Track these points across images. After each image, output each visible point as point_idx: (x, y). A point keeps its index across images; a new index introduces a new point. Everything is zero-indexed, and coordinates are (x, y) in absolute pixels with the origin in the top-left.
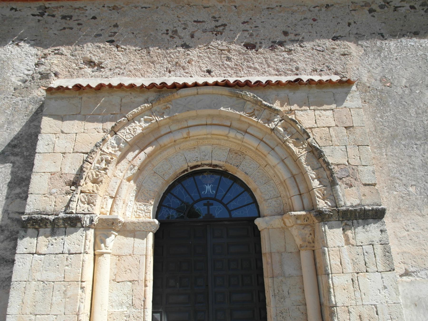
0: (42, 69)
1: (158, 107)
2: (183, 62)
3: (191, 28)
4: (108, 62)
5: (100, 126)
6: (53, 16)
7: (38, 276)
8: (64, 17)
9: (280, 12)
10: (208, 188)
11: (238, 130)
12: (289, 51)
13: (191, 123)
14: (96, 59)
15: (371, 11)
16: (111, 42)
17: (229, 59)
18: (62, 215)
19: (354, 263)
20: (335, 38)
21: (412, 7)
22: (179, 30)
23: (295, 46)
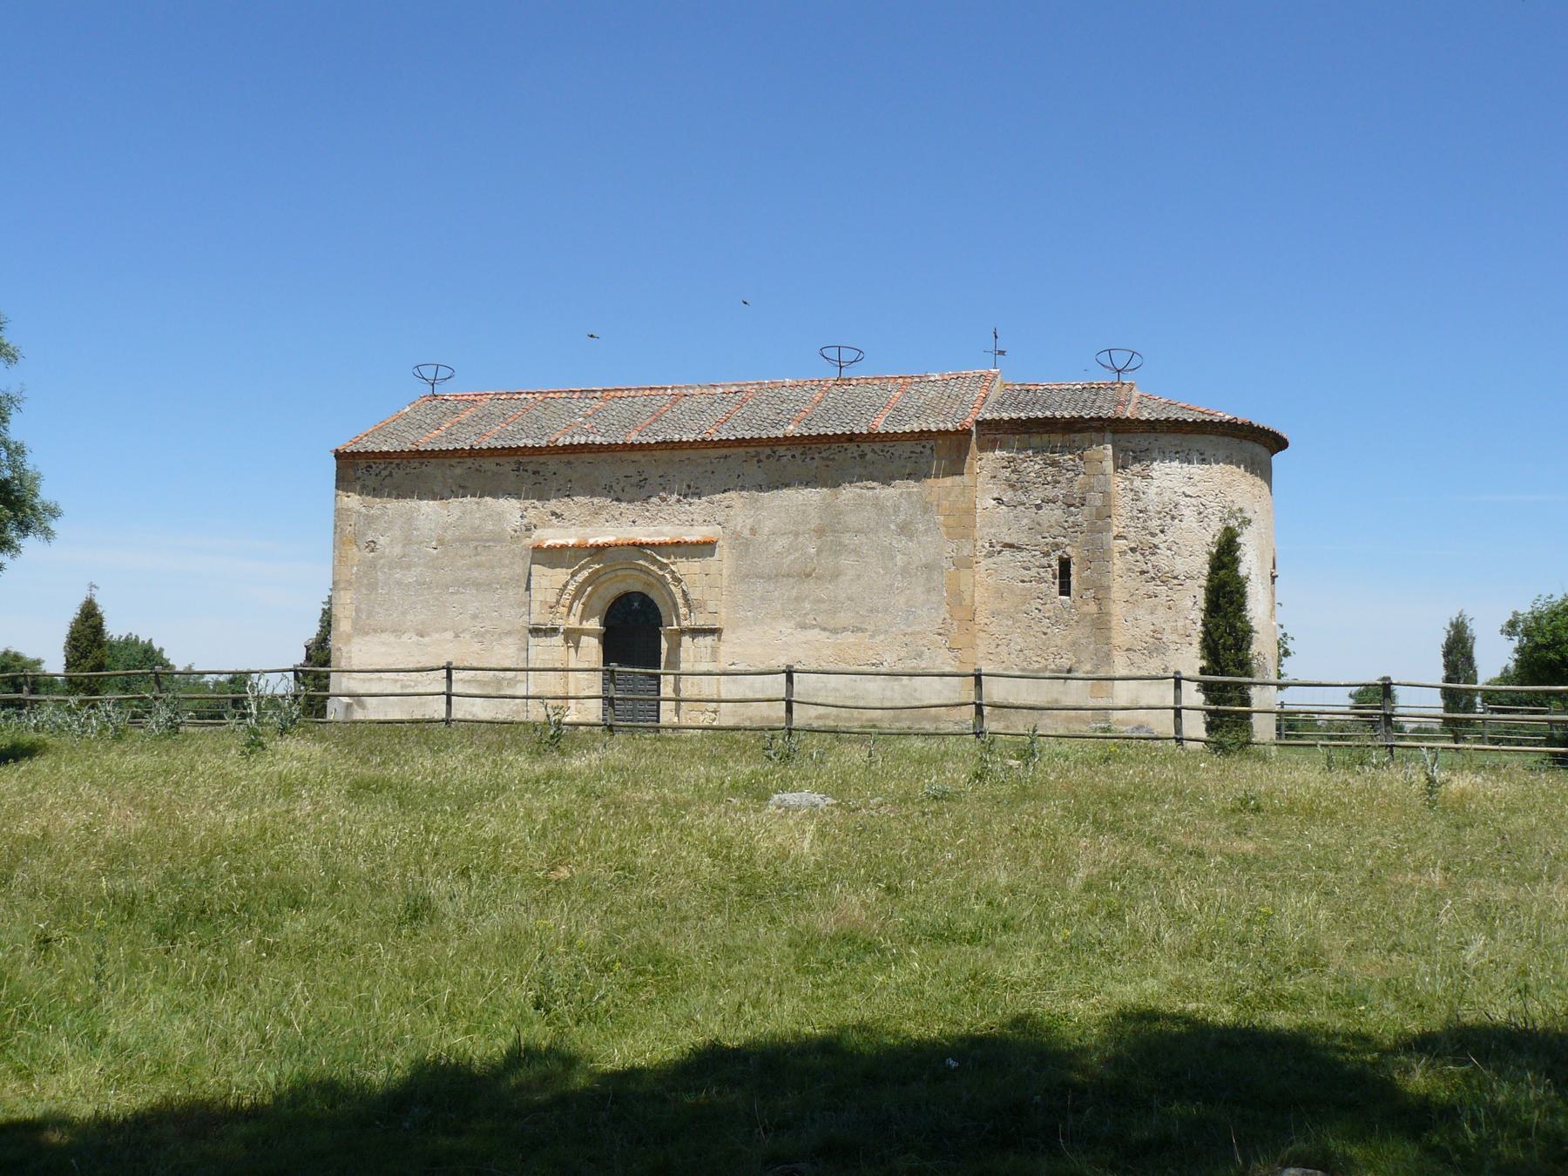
0: (525, 521)
1: (597, 558)
2: (617, 514)
3: (622, 484)
4: (566, 514)
5: (564, 570)
6: (527, 471)
7: (540, 657)
8: (534, 473)
9: (687, 465)
10: (636, 604)
11: (645, 572)
12: (690, 504)
13: (618, 567)
14: (558, 511)
15: (759, 461)
16: (568, 496)
17: (648, 511)
18: (549, 626)
19: (695, 657)
21: (793, 456)
22: (614, 484)
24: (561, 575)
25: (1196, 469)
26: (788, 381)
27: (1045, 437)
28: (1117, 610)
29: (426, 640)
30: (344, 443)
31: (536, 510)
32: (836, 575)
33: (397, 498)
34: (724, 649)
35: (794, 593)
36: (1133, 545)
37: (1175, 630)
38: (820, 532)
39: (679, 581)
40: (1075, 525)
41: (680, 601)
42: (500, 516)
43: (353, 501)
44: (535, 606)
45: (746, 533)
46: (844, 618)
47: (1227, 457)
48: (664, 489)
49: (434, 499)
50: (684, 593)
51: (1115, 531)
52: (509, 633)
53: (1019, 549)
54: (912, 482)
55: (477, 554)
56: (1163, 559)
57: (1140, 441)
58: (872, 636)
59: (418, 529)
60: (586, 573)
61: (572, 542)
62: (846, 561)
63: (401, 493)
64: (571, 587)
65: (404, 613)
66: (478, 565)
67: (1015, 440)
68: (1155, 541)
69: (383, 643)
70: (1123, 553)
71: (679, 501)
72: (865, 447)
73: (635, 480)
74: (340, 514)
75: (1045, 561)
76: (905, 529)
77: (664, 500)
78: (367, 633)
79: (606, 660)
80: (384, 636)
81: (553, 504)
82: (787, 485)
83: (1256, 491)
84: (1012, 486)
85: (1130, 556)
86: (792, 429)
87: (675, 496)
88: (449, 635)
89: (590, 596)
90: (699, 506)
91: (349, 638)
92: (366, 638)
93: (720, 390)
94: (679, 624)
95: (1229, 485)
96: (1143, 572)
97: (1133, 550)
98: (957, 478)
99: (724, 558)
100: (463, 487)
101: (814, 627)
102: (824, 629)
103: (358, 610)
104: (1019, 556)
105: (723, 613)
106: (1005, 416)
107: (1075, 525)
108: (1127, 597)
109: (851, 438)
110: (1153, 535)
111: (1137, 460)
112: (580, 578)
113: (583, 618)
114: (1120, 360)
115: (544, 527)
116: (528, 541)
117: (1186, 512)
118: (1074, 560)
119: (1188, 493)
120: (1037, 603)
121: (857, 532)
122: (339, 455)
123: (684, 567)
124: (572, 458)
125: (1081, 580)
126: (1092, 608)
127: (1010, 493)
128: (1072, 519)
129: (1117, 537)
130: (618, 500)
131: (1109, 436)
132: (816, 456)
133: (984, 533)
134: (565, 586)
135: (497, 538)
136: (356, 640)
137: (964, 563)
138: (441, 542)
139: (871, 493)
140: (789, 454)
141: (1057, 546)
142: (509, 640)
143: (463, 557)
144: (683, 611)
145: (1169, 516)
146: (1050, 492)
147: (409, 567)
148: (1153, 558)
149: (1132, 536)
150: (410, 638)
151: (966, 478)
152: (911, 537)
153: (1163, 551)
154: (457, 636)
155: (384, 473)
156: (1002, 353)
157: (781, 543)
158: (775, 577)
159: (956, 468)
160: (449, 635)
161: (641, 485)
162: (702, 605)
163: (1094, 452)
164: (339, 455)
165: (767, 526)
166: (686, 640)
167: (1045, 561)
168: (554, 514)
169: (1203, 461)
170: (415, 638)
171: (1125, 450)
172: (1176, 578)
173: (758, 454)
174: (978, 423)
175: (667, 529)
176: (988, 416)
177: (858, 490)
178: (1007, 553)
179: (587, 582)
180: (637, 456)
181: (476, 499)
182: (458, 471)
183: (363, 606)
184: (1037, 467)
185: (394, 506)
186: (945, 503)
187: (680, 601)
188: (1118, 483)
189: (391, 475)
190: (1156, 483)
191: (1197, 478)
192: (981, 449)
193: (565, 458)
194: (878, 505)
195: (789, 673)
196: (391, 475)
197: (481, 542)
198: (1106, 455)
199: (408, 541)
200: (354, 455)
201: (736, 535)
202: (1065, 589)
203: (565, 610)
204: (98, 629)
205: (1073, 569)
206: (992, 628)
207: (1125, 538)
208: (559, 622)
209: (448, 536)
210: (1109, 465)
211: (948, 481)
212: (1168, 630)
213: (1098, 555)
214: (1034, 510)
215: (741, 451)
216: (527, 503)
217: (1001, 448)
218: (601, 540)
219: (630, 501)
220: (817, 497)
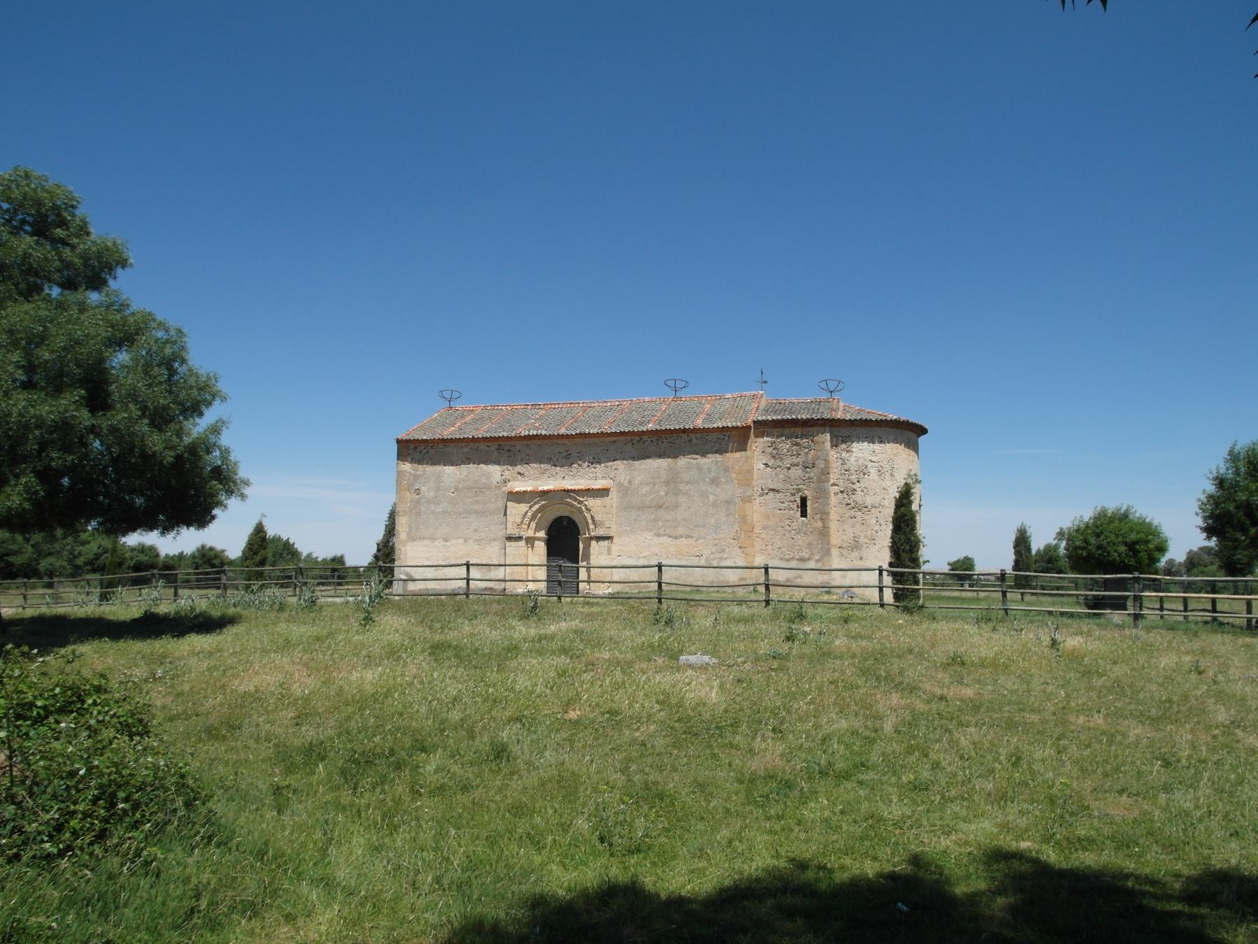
0: (503, 477)
1: (543, 498)
4: (526, 474)
20: (614, 461)
23: (598, 466)
24: (523, 507)
25: (877, 447)
26: (647, 399)
27: (792, 430)
28: (833, 525)
29: (449, 543)
30: (402, 435)
31: (509, 471)
32: (676, 507)
33: (431, 465)
34: (614, 547)
35: (653, 516)
36: (842, 489)
37: (866, 536)
38: (667, 483)
39: (589, 510)
40: (809, 478)
41: (590, 521)
42: (489, 475)
43: (407, 467)
44: (509, 525)
45: (626, 484)
46: (681, 530)
48: (580, 460)
49: (452, 465)
50: (592, 517)
51: (832, 481)
52: (495, 540)
53: (778, 491)
54: (718, 455)
55: (477, 496)
56: (859, 497)
57: (845, 431)
58: (696, 541)
59: (443, 482)
60: (537, 506)
61: (529, 489)
62: (682, 499)
63: (434, 462)
64: (529, 514)
65: (436, 529)
66: (477, 502)
67: (775, 432)
68: (855, 487)
69: (425, 546)
70: (836, 494)
71: (588, 466)
72: (692, 436)
73: (564, 454)
74: (400, 474)
75: (792, 498)
76: (714, 481)
77: (580, 465)
78: (416, 540)
79: (548, 555)
80: (425, 542)
81: (519, 468)
82: (648, 457)
84: (773, 457)
85: (840, 496)
86: (650, 426)
87: (587, 464)
88: (461, 541)
89: (540, 519)
90: (600, 469)
91: (405, 544)
92: (416, 543)
93: (609, 404)
94: (589, 534)
96: (847, 504)
97: (842, 492)
98: (743, 453)
99: (614, 498)
100: (468, 459)
101: (664, 535)
102: (670, 537)
103: (410, 527)
104: (778, 495)
105: (614, 527)
106: (769, 418)
107: (809, 478)
108: (839, 518)
109: (684, 431)
110: (853, 483)
111: (844, 442)
112: (534, 509)
113: (536, 530)
114: (832, 386)
115: (514, 480)
116: (504, 489)
117: (872, 470)
118: (809, 498)
120: (788, 522)
121: (688, 483)
122: (399, 442)
123: (591, 502)
124: (529, 442)
125: (812, 510)
126: (819, 524)
127: (772, 461)
128: (807, 475)
129: (833, 485)
130: (555, 466)
131: (828, 429)
132: (665, 441)
133: (757, 484)
134: (526, 513)
135: (488, 487)
136: (409, 544)
137: (747, 500)
138: (457, 489)
139: (695, 461)
140: (650, 440)
141: (799, 490)
142: (495, 543)
143: (469, 498)
144: (592, 527)
146: (795, 460)
147: (438, 504)
148: (853, 496)
149: (841, 482)
150: (438, 543)
151: (748, 453)
152: (717, 486)
153: (859, 492)
154: (466, 541)
155: (424, 451)
156: (765, 382)
157: (645, 489)
158: (642, 508)
159: (742, 447)
160: (461, 541)
161: (568, 456)
162: (602, 523)
163: (819, 438)
164: (399, 442)
165: (638, 480)
166: (593, 543)
167: (792, 498)
168: (519, 473)
169: (881, 442)
170: (442, 542)
171: (837, 437)
172: (866, 507)
173: (632, 440)
174: (754, 422)
175: (582, 481)
176: (760, 418)
177: (688, 460)
178: (771, 494)
179: (538, 511)
180: (565, 441)
181: (475, 466)
182: (466, 450)
183: (413, 525)
184: (788, 446)
185: (430, 469)
186: (737, 467)
187: (590, 521)
188: (833, 454)
189: (428, 452)
192: (756, 436)
193: (525, 442)
194: (699, 468)
195: (660, 567)
196: (428, 452)
197: (480, 489)
198: (826, 440)
199: (438, 489)
200: (408, 441)
201: (620, 485)
202: (804, 514)
203: (525, 527)
204: (264, 539)
205: (809, 503)
206: (763, 536)
207: (837, 485)
208: (522, 533)
209: (460, 486)
210: (828, 445)
211: (738, 455)
212: (862, 536)
213: (822, 495)
214: (786, 470)
215: (623, 438)
216: (504, 467)
217: (767, 436)
218: (546, 488)
219: (562, 466)
220: (665, 464)
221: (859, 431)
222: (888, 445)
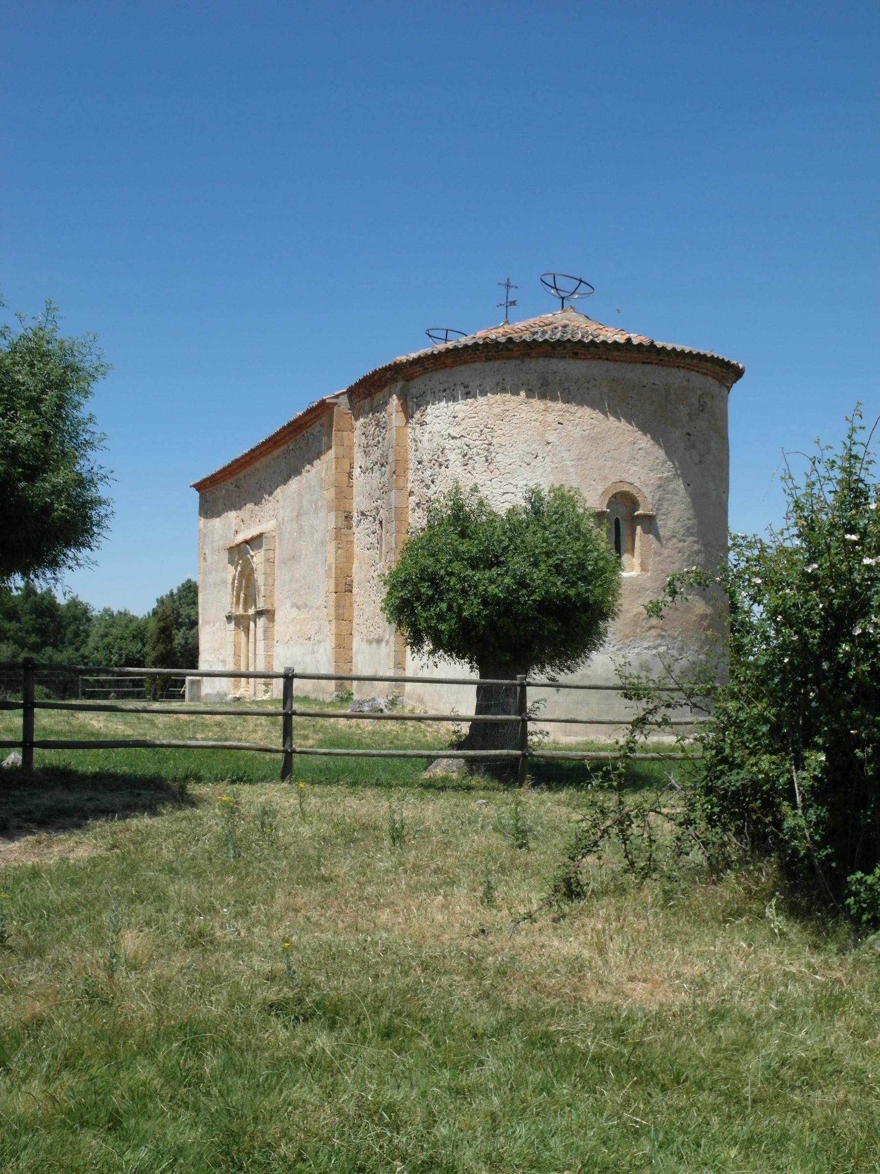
25: (461, 407)
47: (498, 384)
83: (551, 417)
95: (501, 417)
117: (452, 456)
119: (453, 434)
145: (437, 464)
156: (513, 303)
169: (468, 395)
190: (428, 428)
191: (461, 415)
221: (438, 378)
222: (481, 399)
